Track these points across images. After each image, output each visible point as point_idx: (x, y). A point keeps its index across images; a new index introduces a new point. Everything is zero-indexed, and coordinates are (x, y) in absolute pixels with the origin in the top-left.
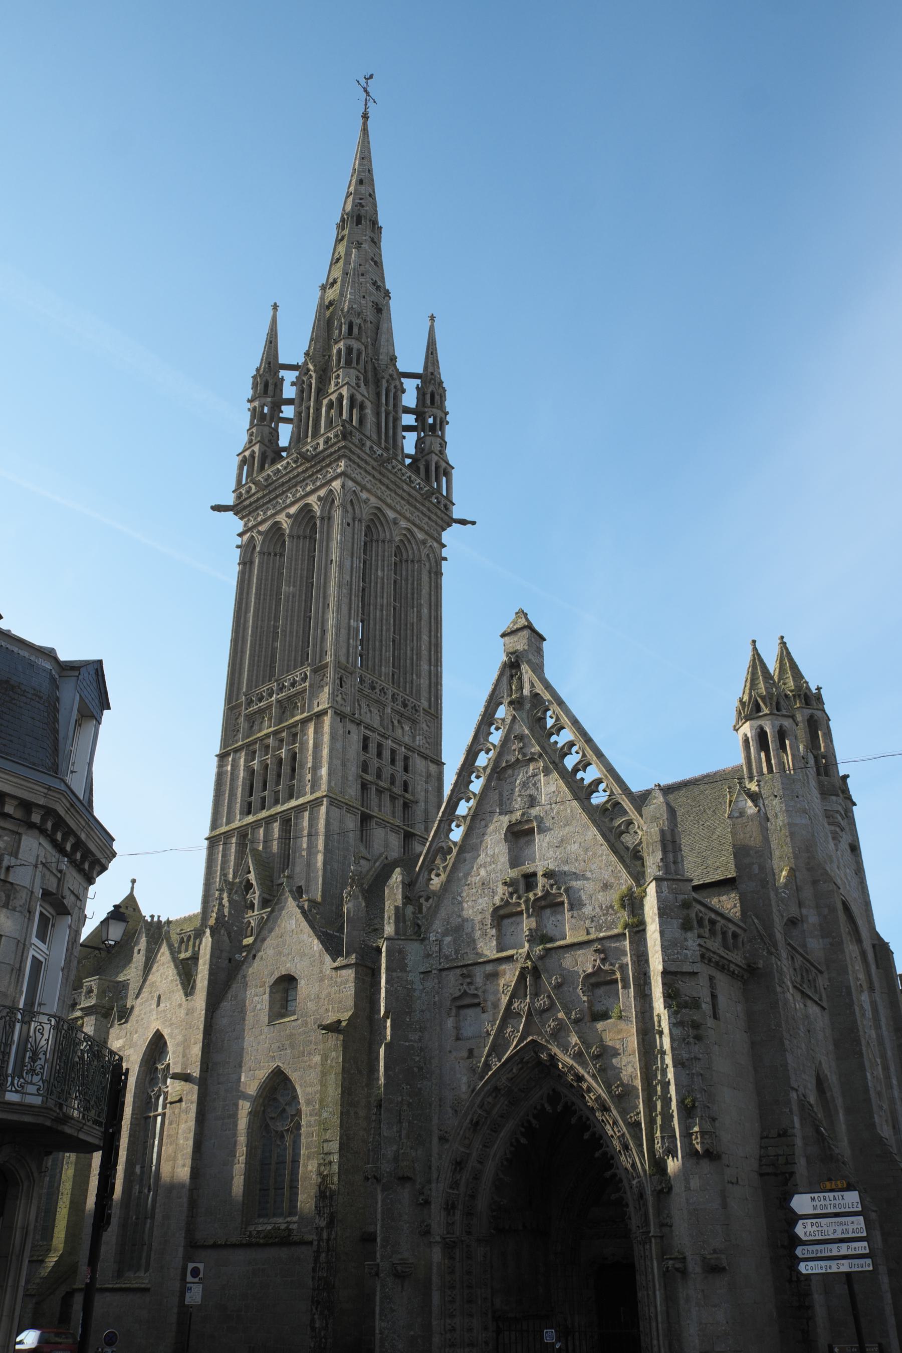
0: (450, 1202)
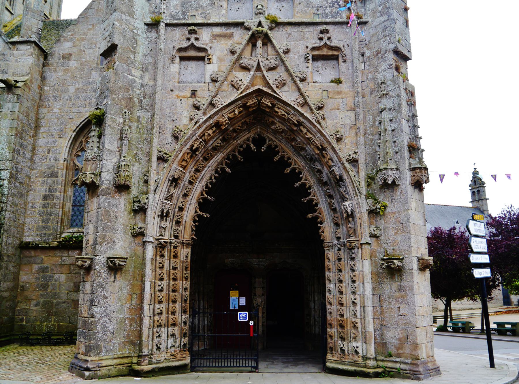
0: (166, 211)
